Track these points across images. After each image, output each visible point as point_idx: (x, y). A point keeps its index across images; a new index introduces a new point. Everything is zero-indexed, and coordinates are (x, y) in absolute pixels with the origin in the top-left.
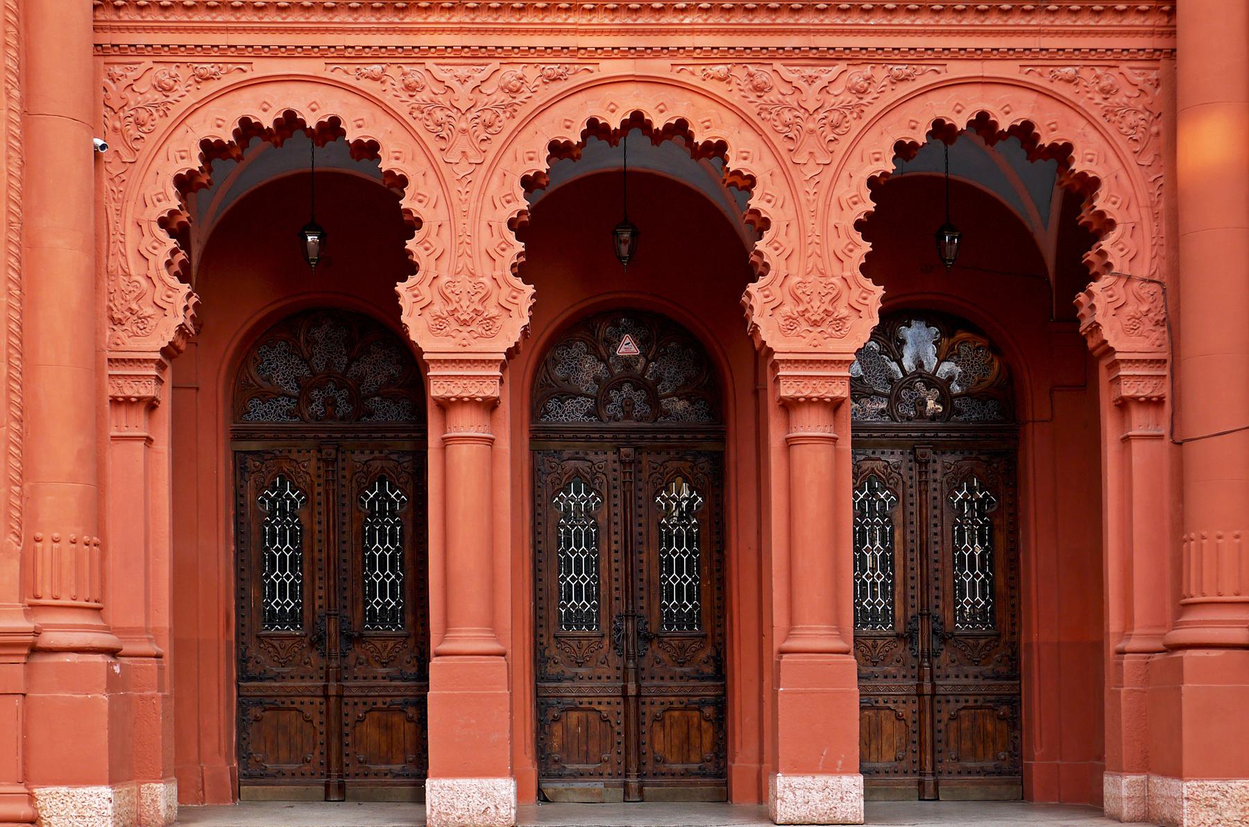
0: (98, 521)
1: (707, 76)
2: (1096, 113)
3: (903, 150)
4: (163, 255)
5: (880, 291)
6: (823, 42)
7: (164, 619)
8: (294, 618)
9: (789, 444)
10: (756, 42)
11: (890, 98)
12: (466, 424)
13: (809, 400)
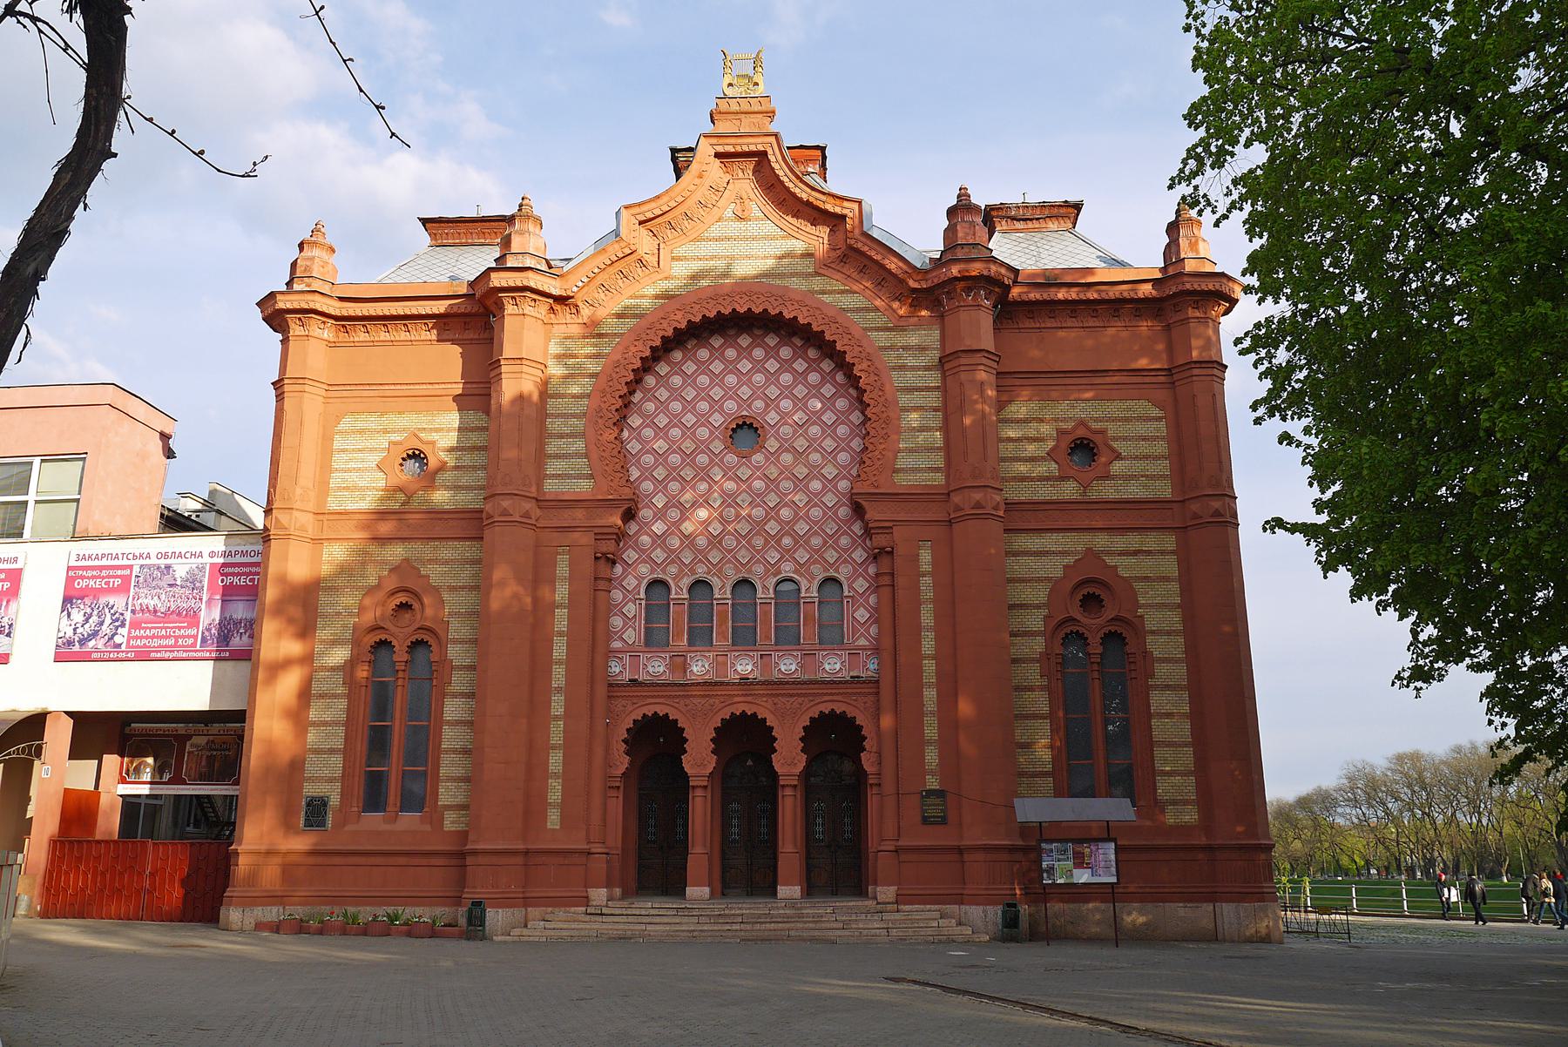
0: (604, 820)
1: (763, 701)
2: (862, 709)
4: (623, 749)
6: (791, 692)
7: (620, 846)
8: (654, 842)
9: (783, 796)
10: (774, 692)
11: (808, 706)
12: (699, 792)
13: (787, 785)
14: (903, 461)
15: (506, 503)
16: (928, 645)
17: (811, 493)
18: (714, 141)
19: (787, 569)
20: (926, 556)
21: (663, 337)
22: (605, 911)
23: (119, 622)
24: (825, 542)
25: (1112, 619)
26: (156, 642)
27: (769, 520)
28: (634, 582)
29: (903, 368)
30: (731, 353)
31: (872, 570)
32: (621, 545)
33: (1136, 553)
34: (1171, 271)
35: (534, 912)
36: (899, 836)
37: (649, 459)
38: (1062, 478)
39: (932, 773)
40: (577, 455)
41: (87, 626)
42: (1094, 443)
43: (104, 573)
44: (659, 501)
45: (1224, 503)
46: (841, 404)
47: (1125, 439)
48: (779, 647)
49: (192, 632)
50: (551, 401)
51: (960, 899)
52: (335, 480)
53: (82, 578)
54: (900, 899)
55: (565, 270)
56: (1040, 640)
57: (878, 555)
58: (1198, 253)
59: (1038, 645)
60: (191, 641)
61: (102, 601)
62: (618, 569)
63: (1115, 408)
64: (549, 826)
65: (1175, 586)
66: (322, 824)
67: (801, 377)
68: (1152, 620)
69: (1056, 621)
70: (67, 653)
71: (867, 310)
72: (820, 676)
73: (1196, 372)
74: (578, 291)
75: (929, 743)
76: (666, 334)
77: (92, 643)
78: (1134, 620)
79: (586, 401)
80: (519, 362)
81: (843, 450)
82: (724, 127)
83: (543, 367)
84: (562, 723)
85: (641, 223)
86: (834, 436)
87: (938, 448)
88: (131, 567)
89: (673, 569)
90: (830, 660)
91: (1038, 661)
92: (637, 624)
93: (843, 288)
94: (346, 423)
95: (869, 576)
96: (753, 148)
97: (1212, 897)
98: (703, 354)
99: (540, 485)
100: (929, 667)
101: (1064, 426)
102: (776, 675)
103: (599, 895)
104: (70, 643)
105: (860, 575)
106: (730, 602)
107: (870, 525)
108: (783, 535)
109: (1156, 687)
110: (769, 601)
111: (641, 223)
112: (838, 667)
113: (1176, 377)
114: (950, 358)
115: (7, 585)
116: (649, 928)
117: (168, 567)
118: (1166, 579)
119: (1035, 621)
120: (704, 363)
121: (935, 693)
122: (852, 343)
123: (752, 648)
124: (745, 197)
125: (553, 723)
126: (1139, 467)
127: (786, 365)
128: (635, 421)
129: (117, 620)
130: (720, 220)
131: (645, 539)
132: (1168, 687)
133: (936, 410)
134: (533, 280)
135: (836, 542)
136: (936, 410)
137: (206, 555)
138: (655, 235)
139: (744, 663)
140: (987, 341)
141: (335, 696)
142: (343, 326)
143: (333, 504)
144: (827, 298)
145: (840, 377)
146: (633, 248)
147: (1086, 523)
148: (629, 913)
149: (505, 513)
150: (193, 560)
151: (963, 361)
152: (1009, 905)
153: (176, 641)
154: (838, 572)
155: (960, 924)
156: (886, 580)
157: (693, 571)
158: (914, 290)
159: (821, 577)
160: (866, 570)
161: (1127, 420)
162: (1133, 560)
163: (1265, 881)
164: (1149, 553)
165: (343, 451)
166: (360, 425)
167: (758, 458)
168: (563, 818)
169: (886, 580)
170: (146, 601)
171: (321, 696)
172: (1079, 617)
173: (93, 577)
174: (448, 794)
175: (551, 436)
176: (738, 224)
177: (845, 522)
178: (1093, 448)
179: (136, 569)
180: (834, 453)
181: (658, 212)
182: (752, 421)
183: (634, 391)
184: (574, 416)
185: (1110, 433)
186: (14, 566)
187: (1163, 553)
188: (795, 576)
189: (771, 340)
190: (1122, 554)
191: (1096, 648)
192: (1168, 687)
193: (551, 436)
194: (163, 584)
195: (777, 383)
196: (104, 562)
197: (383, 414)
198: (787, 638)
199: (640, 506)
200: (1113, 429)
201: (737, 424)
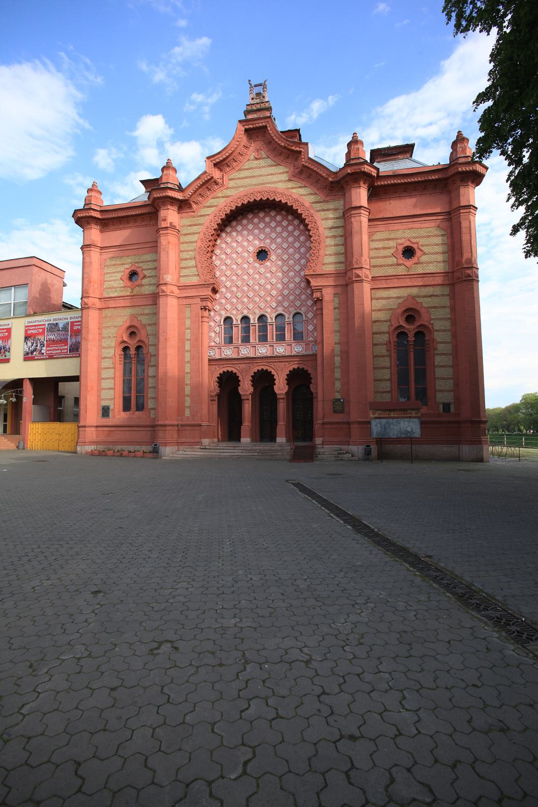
5: (287, 387)
15: (164, 288)
18: (244, 124)
19: (280, 310)
21: (226, 214)
22: (207, 447)
23: (42, 345)
24: (296, 298)
25: (419, 325)
26: (55, 352)
27: (272, 290)
29: (326, 219)
30: (256, 220)
31: (315, 309)
32: (213, 303)
33: (431, 296)
34: (452, 163)
35: (181, 447)
36: (324, 417)
38: (398, 265)
39: (338, 392)
40: (192, 267)
41: (33, 347)
42: (413, 248)
43: (37, 328)
44: (228, 284)
45: (472, 272)
46: (302, 238)
47: (428, 245)
49: (66, 347)
50: (181, 246)
52: (106, 285)
53: (30, 330)
56: (387, 335)
58: (466, 154)
59: (385, 338)
60: (66, 350)
61: (37, 338)
62: (212, 313)
63: (423, 232)
64: (186, 415)
65: (448, 310)
67: (285, 228)
68: (437, 325)
69: (393, 328)
70: (28, 357)
73: (461, 211)
74: (190, 197)
75: (337, 379)
77: (35, 353)
78: (429, 325)
81: (303, 258)
82: (250, 117)
83: (177, 231)
86: (299, 253)
87: (342, 253)
88: (45, 325)
90: (298, 347)
91: (386, 344)
96: (260, 125)
97: (458, 443)
98: (245, 222)
101: (400, 241)
103: (206, 441)
104: (28, 354)
105: (310, 311)
106: (257, 325)
107: (313, 288)
109: (438, 354)
113: (452, 215)
114: (347, 211)
115: (7, 334)
116: (222, 454)
117: (57, 324)
118: (444, 307)
119: (385, 328)
120: (245, 226)
122: (305, 209)
123: (266, 343)
126: (433, 257)
127: (279, 224)
128: (217, 251)
129: (42, 344)
130: (248, 160)
131: (223, 301)
132: (443, 354)
133: (341, 236)
134: (171, 193)
135: (300, 298)
136: (341, 236)
137: (69, 318)
138: (221, 170)
140: (364, 201)
141: (109, 368)
144: (294, 191)
145: (302, 227)
146: (211, 176)
147: (409, 284)
148: (217, 448)
149: (163, 291)
150: (65, 321)
151: (353, 212)
152: (367, 446)
153: (61, 351)
155: (346, 453)
156: (319, 312)
158: (332, 182)
160: (313, 309)
161: (428, 236)
162: (429, 299)
163: (483, 436)
164: (437, 296)
167: (268, 264)
168: (191, 412)
169: (319, 312)
170: (50, 337)
171: (106, 368)
172: (404, 325)
173: (33, 329)
174: (150, 404)
175: (182, 260)
177: (304, 289)
178: (413, 250)
179: (47, 325)
180: (299, 260)
182: (265, 248)
184: (191, 251)
185: (421, 243)
186: (8, 327)
187: (443, 295)
189: (273, 213)
190: (424, 297)
191: (411, 338)
192: (443, 354)
193: (182, 260)
194: (55, 330)
195: (275, 231)
196: (36, 324)
197: (121, 257)
200: (422, 241)
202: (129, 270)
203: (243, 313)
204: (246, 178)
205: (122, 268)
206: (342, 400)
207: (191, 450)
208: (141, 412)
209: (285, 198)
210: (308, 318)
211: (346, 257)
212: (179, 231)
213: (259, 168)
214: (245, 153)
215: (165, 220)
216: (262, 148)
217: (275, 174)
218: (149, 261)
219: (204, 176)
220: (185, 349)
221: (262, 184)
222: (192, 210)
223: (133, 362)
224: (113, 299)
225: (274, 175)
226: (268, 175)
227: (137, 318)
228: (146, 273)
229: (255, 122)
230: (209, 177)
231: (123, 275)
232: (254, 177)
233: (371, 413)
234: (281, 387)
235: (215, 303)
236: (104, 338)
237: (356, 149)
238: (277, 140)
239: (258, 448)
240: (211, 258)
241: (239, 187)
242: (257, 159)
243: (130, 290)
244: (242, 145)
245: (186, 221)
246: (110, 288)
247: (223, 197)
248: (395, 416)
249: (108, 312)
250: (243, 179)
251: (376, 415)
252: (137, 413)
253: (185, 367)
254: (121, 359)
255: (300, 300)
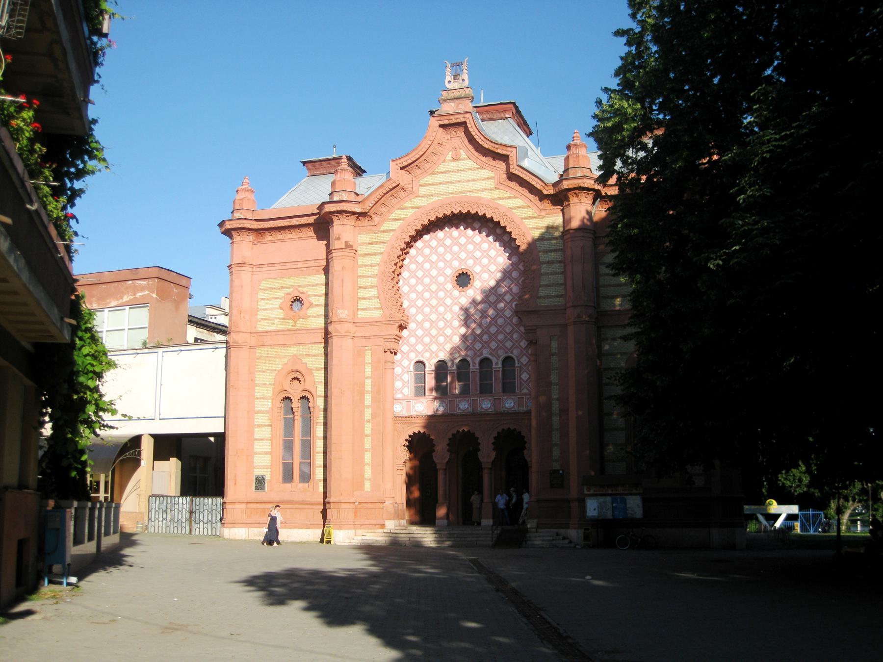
3: (498, 433)
14: (543, 292)
16: (555, 393)
17: (498, 310)
19: (486, 353)
20: (554, 345)
24: (506, 337)
28: (408, 363)
32: (401, 342)
37: (413, 296)
40: (374, 297)
44: (420, 318)
48: (481, 395)
50: (359, 269)
51: (567, 526)
52: (261, 315)
54: (538, 526)
55: (366, 195)
57: (531, 343)
62: (399, 356)
64: (366, 490)
66: (263, 489)
71: (523, 207)
72: (502, 410)
76: (417, 228)
79: (377, 268)
80: (341, 250)
83: (354, 251)
84: (370, 438)
85: (402, 168)
89: (427, 355)
90: (509, 402)
92: (409, 385)
93: (510, 195)
94: (264, 285)
95: (528, 354)
96: (459, 121)
99: (355, 314)
100: (556, 406)
102: (479, 409)
108: (483, 335)
110: (476, 370)
111: (402, 168)
112: (512, 404)
121: (558, 419)
124: (457, 146)
125: (367, 438)
128: (405, 274)
130: (444, 161)
133: (560, 262)
135: (512, 337)
136: (560, 262)
139: (463, 404)
141: (265, 426)
142: (259, 233)
143: (260, 329)
144: (501, 202)
146: (398, 183)
154: (513, 354)
155: (564, 538)
157: (437, 356)
159: (502, 357)
160: (527, 352)
165: (263, 299)
166: (270, 286)
171: (259, 426)
175: (360, 288)
176: (453, 164)
177: (516, 325)
181: (410, 162)
183: (404, 259)
188: (490, 357)
193: (360, 288)
198: (485, 390)
199: (409, 321)
201: (459, 274)
202: (290, 297)
203: (437, 357)
204: (440, 183)
205: (281, 294)
206: (561, 472)
207: (371, 534)
208: (306, 485)
209: (490, 212)
210: (522, 363)
211: (566, 289)
212: (356, 251)
213: (458, 171)
214: (441, 152)
215: (338, 239)
216: (461, 147)
217: (478, 180)
218: (317, 285)
219: (388, 183)
220: (364, 403)
221: (464, 192)
222: (373, 224)
223: (296, 418)
224: (269, 334)
225: (476, 180)
226: (468, 181)
227: (301, 360)
228: (312, 300)
229: (452, 117)
230: (394, 185)
231: (283, 302)
232: (451, 183)
233: (585, 487)
234: (487, 454)
235: (403, 342)
236: (258, 386)
237: (575, 156)
238: (478, 140)
239: (456, 532)
240: (397, 283)
241: (431, 195)
242: (455, 160)
243: (291, 322)
244: (436, 142)
245: (363, 238)
246: (265, 319)
247: (412, 208)
248: (614, 492)
249: (261, 352)
250: (438, 185)
251: (592, 492)
252: (302, 485)
253: (364, 427)
254: (279, 414)
255: (511, 339)
